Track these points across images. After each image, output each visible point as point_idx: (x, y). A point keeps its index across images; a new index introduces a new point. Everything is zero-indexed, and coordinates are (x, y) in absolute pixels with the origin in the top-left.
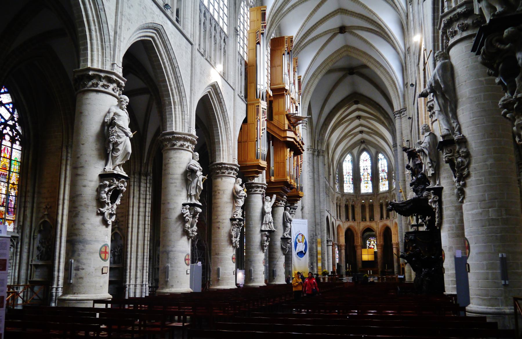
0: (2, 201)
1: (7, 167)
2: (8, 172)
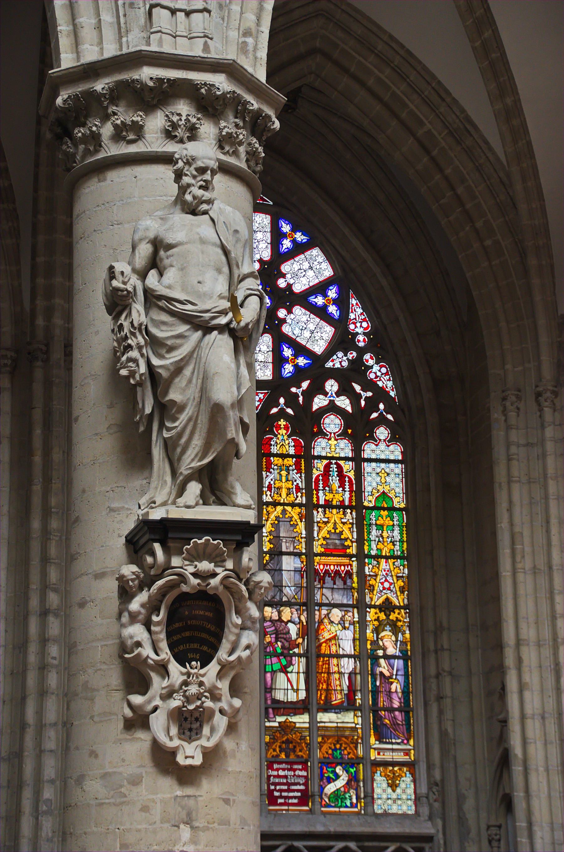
0: (345, 688)
1: (348, 543)
2: (355, 564)
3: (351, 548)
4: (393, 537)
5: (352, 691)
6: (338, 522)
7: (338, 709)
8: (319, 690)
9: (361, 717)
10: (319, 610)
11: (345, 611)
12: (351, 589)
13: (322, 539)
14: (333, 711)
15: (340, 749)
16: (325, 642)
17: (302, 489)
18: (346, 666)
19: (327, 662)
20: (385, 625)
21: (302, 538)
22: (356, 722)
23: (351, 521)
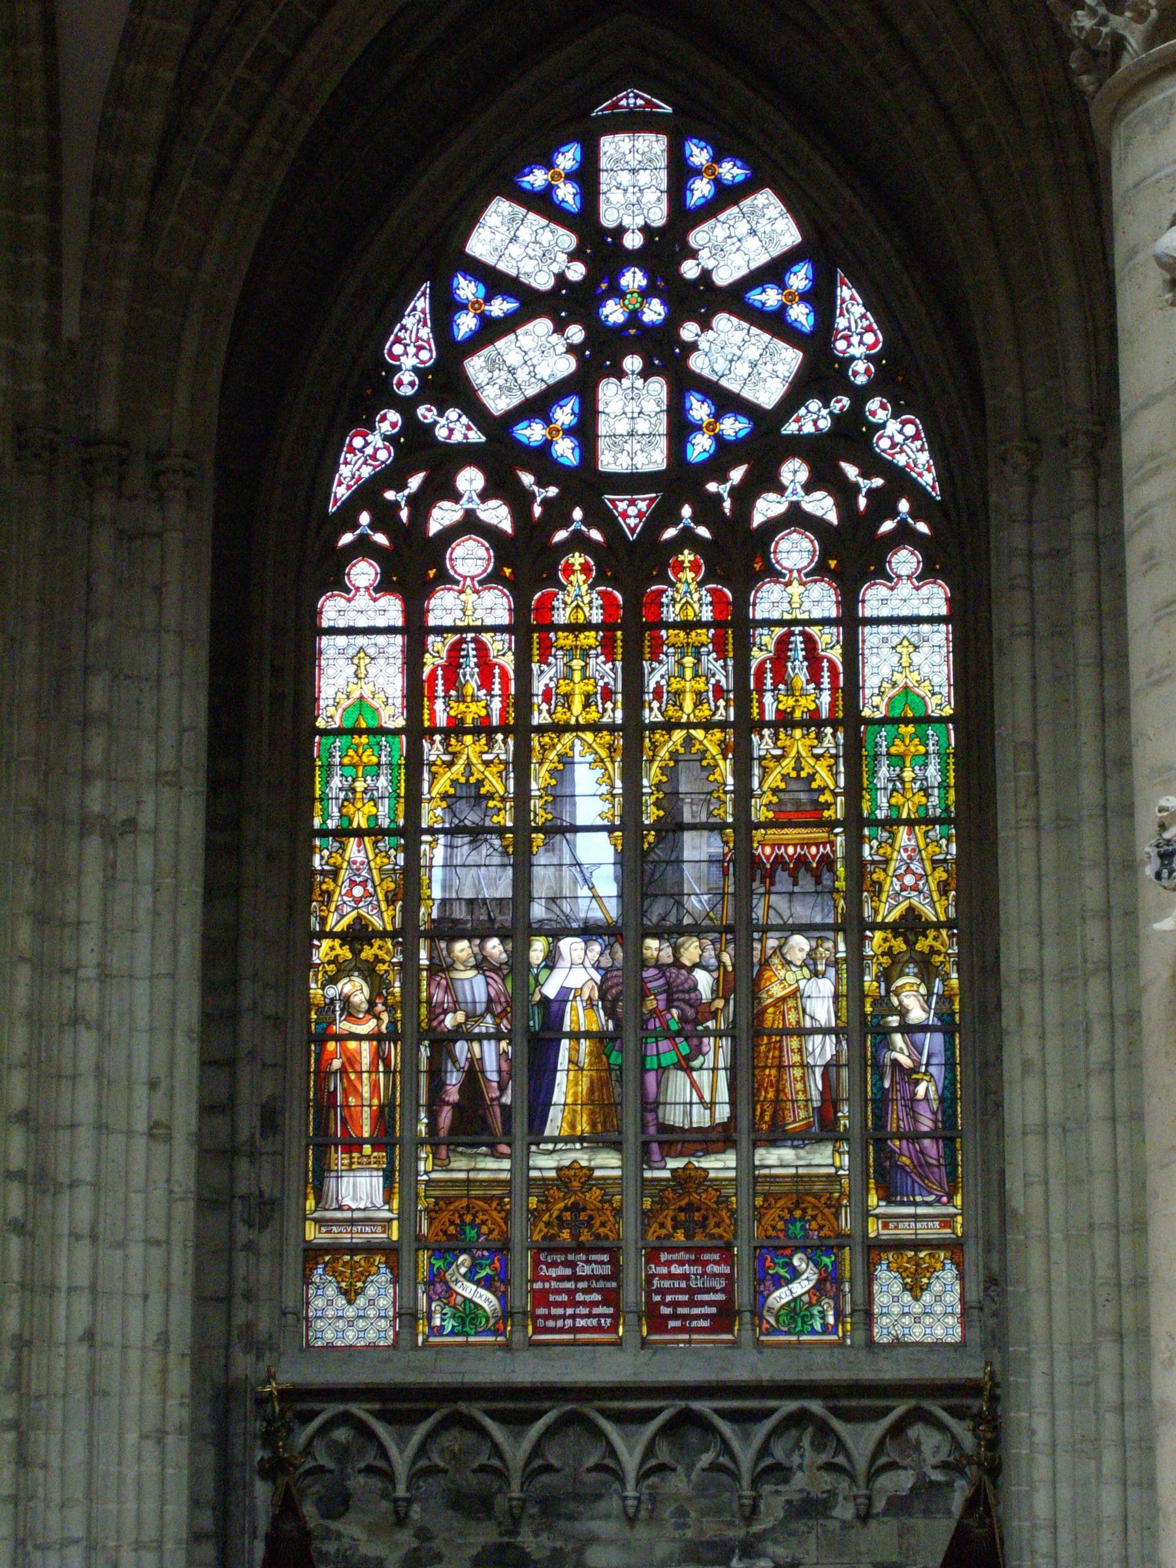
0: (815, 1095)
1: (826, 797)
3: (833, 807)
4: (926, 779)
6: (804, 754)
8: (758, 1101)
9: (848, 1152)
10: (760, 940)
12: (831, 893)
13: (769, 793)
14: (789, 1143)
15: (802, 1218)
16: (774, 1005)
17: (728, 691)
18: (817, 1052)
21: (725, 792)
22: (838, 1163)
23: (833, 751)
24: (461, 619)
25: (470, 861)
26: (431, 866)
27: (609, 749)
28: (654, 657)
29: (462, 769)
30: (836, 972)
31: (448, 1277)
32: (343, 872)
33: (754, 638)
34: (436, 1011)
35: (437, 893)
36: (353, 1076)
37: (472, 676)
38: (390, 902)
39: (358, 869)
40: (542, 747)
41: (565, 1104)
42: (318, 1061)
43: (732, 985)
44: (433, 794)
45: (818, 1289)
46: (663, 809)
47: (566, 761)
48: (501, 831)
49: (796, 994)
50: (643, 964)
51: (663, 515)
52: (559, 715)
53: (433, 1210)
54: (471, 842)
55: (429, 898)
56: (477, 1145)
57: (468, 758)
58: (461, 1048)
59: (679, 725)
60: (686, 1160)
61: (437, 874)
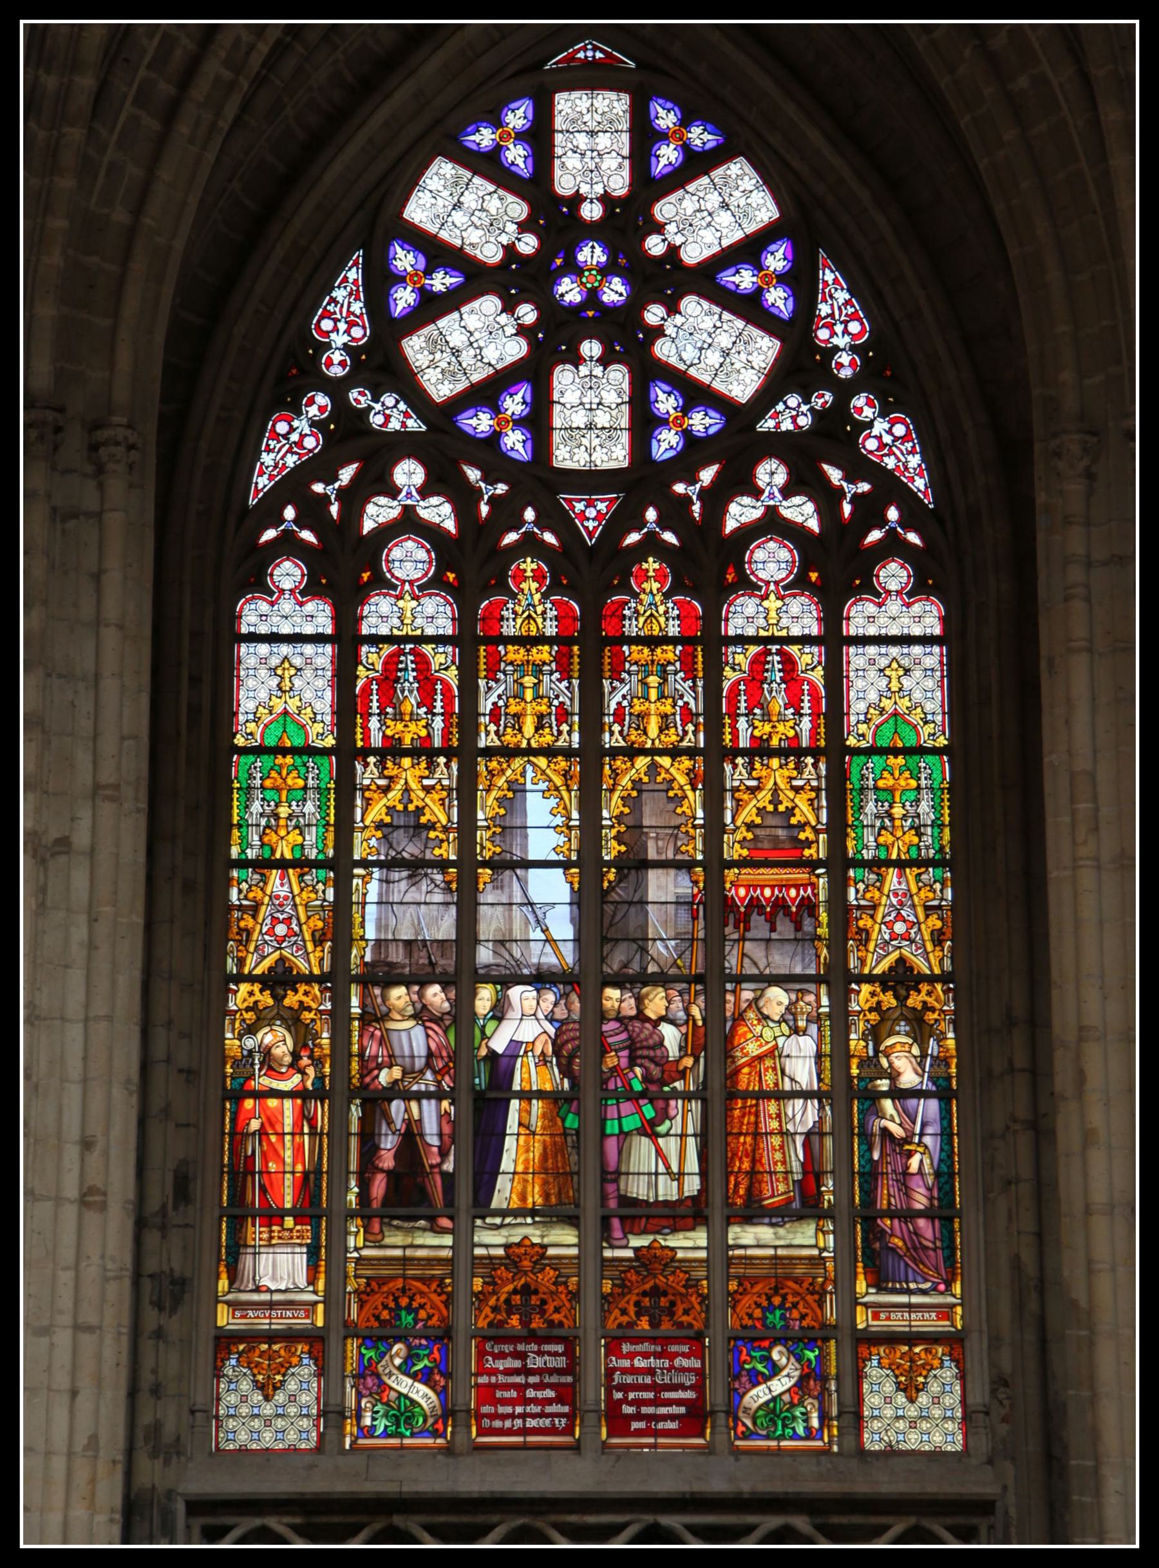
0: (796, 1167)
3: (814, 845)
4: (918, 816)
5: (812, 1171)
6: (782, 787)
7: (777, 1216)
8: (732, 1172)
9: (834, 1232)
10: (734, 992)
11: (799, 990)
12: (813, 940)
13: (743, 829)
14: (766, 1220)
17: (698, 715)
18: (798, 1117)
19: (753, 1110)
20: (896, 1021)
21: (694, 827)
22: (821, 1244)
23: (814, 783)
24: (398, 629)
25: (408, 898)
26: (364, 904)
27: (564, 775)
28: (616, 676)
29: (399, 796)
30: (819, 1029)
31: (380, 1369)
32: (263, 908)
33: (727, 657)
34: (369, 1066)
35: (371, 933)
36: (273, 1138)
37: (411, 692)
38: (318, 942)
39: (281, 905)
40: (490, 772)
41: (514, 1173)
42: (234, 1120)
43: (702, 1041)
44: (367, 823)
45: (801, 1385)
46: (625, 844)
47: (517, 789)
48: (442, 865)
49: (774, 1053)
50: (603, 1017)
51: (626, 518)
52: (508, 737)
53: (363, 1293)
54: (410, 877)
55: (362, 938)
56: (416, 1218)
57: (406, 783)
58: (397, 1108)
59: (643, 752)
60: (651, 1238)
61: (371, 911)
